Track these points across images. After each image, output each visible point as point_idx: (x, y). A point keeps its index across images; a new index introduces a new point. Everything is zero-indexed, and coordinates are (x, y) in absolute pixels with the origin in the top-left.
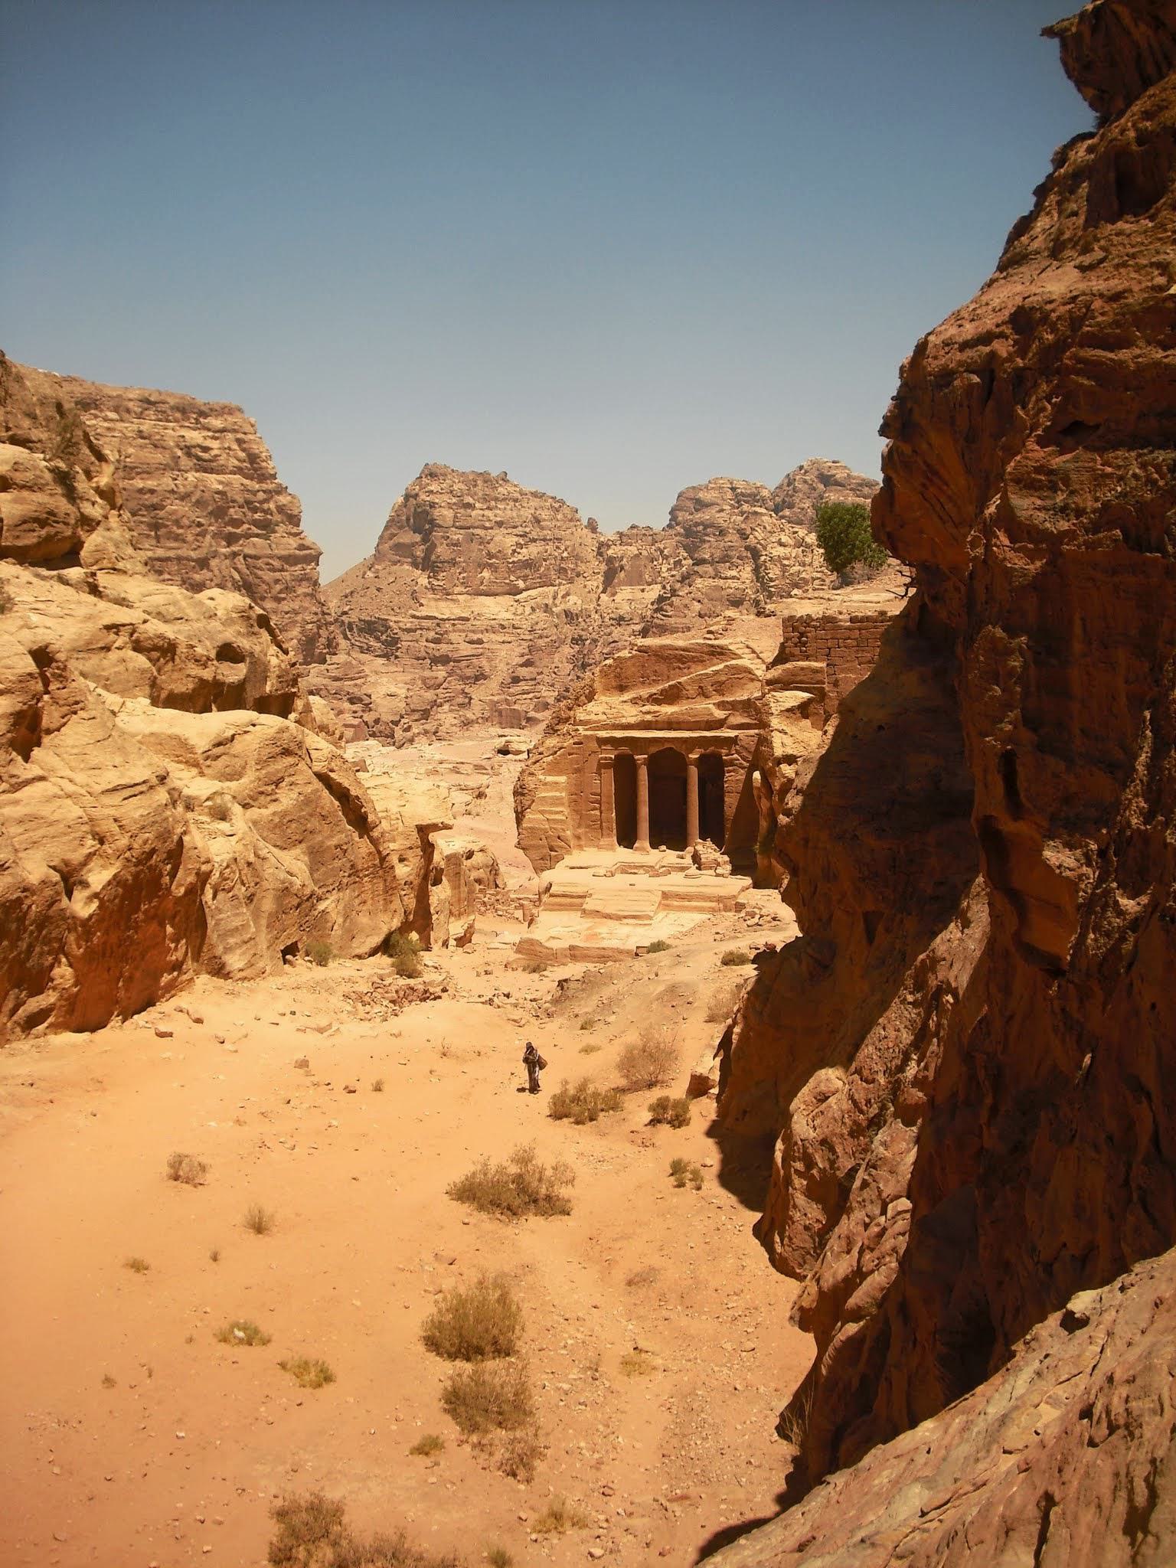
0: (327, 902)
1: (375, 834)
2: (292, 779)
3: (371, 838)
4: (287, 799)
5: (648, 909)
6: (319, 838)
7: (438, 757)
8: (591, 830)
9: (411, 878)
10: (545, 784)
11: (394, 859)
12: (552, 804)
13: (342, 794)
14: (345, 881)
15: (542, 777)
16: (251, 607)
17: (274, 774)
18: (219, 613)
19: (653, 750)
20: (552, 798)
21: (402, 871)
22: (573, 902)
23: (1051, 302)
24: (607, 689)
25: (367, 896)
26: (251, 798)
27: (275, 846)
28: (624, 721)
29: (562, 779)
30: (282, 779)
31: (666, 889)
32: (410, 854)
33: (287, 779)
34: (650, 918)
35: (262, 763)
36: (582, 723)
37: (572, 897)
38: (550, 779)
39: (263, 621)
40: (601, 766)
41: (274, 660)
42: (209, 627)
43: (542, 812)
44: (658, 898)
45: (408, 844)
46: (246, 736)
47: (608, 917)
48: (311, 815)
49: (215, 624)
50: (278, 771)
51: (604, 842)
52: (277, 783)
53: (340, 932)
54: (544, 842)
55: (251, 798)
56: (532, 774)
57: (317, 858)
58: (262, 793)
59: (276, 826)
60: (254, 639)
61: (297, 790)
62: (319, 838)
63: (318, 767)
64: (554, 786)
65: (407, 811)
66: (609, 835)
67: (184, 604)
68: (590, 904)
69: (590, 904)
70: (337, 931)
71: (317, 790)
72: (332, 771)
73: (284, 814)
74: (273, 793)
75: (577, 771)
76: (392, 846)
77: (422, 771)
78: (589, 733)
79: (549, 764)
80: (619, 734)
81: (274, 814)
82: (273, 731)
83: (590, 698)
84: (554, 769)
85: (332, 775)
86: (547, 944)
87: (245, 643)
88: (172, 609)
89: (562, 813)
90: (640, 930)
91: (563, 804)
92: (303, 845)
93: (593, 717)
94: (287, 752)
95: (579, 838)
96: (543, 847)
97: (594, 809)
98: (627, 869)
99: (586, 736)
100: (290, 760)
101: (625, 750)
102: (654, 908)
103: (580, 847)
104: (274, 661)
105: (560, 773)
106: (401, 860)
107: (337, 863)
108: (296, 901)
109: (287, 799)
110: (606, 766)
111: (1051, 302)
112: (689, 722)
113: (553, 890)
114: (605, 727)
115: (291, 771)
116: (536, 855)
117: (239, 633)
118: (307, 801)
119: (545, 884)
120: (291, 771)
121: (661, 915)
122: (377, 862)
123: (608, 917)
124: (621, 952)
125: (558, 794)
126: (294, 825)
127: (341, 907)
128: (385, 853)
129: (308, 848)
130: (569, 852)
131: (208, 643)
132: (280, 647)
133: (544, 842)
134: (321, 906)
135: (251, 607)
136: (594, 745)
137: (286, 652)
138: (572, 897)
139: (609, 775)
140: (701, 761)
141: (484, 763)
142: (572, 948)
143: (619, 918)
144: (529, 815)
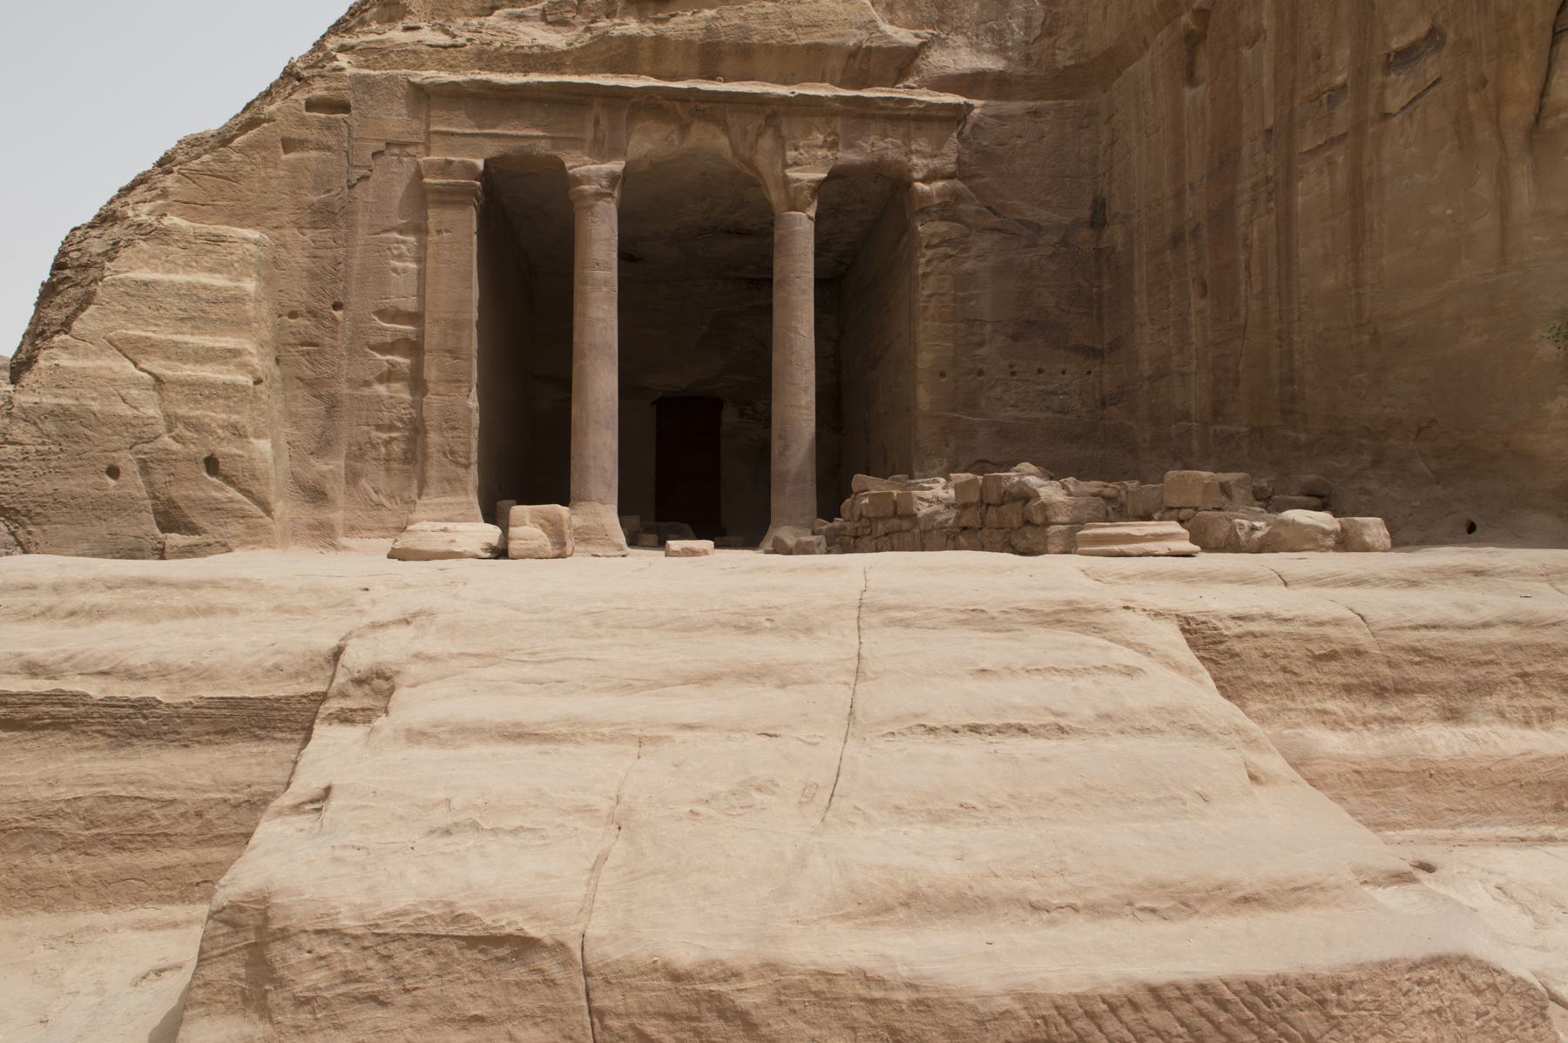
19: (647, 142)
20: (190, 293)
37: (132, 723)
40: (422, 197)
43: (130, 349)
54: (133, 484)
66: (451, 484)
75: (325, 216)
95: (316, 494)
97: (388, 376)
101: (524, 135)
110: (447, 197)
112: (787, 50)
130: (256, 536)
136: (396, 120)
138: (132, 723)
139: (458, 236)
140: (837, 194)
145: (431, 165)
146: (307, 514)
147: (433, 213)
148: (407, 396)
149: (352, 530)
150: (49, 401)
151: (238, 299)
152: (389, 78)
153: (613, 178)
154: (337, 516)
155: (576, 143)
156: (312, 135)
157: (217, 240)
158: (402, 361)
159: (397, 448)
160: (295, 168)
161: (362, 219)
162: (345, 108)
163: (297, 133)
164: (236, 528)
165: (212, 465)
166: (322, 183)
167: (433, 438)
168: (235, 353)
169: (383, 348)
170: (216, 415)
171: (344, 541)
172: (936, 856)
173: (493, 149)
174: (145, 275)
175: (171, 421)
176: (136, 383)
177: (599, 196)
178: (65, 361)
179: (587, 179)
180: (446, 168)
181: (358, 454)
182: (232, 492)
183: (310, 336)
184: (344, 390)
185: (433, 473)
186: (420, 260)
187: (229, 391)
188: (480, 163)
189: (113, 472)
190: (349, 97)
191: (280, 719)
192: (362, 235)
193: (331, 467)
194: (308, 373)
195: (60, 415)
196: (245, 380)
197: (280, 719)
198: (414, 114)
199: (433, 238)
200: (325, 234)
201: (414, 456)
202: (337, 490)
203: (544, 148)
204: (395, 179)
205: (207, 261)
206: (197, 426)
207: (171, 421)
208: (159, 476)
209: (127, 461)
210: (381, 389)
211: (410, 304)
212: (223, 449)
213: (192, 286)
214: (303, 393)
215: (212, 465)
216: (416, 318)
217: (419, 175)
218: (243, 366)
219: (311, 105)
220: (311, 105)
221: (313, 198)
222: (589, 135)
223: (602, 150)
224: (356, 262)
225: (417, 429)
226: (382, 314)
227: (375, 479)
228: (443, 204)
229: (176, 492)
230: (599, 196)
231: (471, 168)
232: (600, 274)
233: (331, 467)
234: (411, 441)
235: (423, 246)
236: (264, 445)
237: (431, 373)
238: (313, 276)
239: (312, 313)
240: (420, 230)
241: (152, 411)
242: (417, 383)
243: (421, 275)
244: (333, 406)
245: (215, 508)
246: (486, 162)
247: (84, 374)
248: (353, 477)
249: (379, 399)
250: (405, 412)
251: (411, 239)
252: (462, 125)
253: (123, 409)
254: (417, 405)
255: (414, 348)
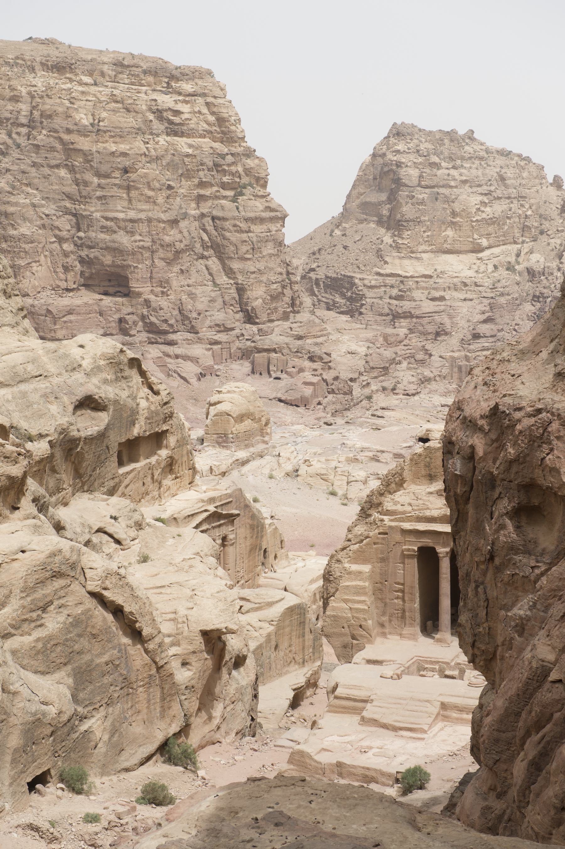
0: (93, 720)
1: (151, 646)
2: (62, 601)
3: (146, 651)
4: (53, 623)
5: (424, 722)
6: (87, 657)
7: (359, 445)
8: (392, 619)
9: (193, 682)
10: (350, 573)
11: (175, 665)
12: (358, 594)
13: (117, 611)
14: (116, 695)
15: (347, 565)
16: (122, 351)
17: (39, 600)
18: (85, 363)
20: (355, 587)
21: (183, 676)
22: (353, 705)
23: (520, 409)
24: (417, 478)
25: (142, 706)
26: (13, 626)
27: (36, 672)
28: (428, 513)
29: (366, 568)
30: (51, 602)
31: (446, 700)
32: (193, 659)
33: (56, 603)
34: (425, 732)
35: (27, 590)
36: (388, 513)
37: (355, 700)
38: (355, 567)
39: (135, 363)
41: (145, 403)
42: (69, 382)
43: (346, 601)
44: (435, 709)
45: (191, 648)
46: (15, 565)
47: (385, 726)
48: (80, 636)
49: (79, 376)
50: (45, 596)
51: (407, 631)
52: (44, 609)
53: (104, 750)
54: (347, 630)
55: (13, 626)
56: (338, 561)
57: (83, 677)
58: (26, 620)
59: (38, 653)
60: (123, 384)
61: (66, 612)
62: (87, 657)
63: (92, 586)
64: (359, 574)
65: (193, 614)
66: (411, 625)
67: (45, 359)
68: (370, 712)
69: (370, 712)
70: (102, 748)
71: (89, 610)
72: (105, 589)
73: (50, 638)
74: (39, 618)
75: (383, 560)
76: (173, 651)
77: (342, 459)
78: (393, 524)
79: (354, 552)
80: (422, 527)
81: (38, 640)
82: (41, 557)
83: (401, 484)
84: (360, 558)
85: (105, 593)
86: (316, 758)
87: (107, 392)
88: (30, 367)
89: (365, 602)
90: (411, 746)
91: (365, 594)
92: (69, 667)
93: (399, 508)
94: (58, 575)
95: (382, 625)
96: (344, 635)
97: (397, 598)
98: (421, 668)
99: (390, 527)
100: (59, 583)
101: (427, 542)
102: (430, 720)
103: (384, 635)
104: (143, 404)
105: (365, 561)
106: (184, 664)
107: (107, 680)
108: (49, 730)
109: (53, 623)
110: (410, 557)
111: (520, 409)
113: (339, 692)
114: (409, 519)
115: (62, 593)
116: (338, 642)
117: (105, 381)
118: (78, 623)
119: (332, 684)
120: (62, 593)
121: (440, 725)
122: (154, 671)
123: (385, 726)
124: (383, 774)
125: (361, 583)
126: (59, 649)
127: (108, 723)
128: (161, 663)
129: (73, 670)
130: (370, 642)
131: (65, 399)
132: (151, 388)
133: (347, 630)
134: (84, 727)
135: (122, 351)
136: (398, 537)
137: (157, 393)
138: (355, 700)
141: (403, 452)
142: (339, 765)
143: (395, 729)
144: (333, 603)
145: (405, 549)
146: (380, 630)
147: (406, 560)
148: (401, 603)
149: (390, 633)
150: (332, 613)
151: (365, 588)
152: (397, 526)
153: (447, 553)
154: (387, 631)
155: (438, 544)
156: (380, 541)
157: (360, 573)
158: (400, 594)
159: (400, 615)
160: (377, 549)
161: (391, 560)
162: (386, 534)
163: (377, 541)
164: (365, 640)
165: (361, 626)
166: (382, 553)
167: (407, 614)
168: (365, 601)
169: (396, 591)
170: (361, 616)
171: (388, 636)
172: (399, 718)
173: (420, 545)
174: (347, 584)
175: (353, 617)
176: (347, 609)
177: (444, 557)
178: (334, 604)
179: (441, 553)
180: (409, 550)
181: (391, 616)
182: (365, 633)
183: (380, 589)
184: (388, 601)
185: (407, 622)
186: (404, 570)
187: (364, 610)
188: (416, 549)
189: (343, 627)
190: (388, 531)
191: (365, 701)
192: (391, 564)
193: (385, 619)
194: (380, 597)
195: (334, 616)
196: (366, 608)
197: (365, 701)
198: (402, 535)
199: (406, 566)
200: (383, 564)
201: (403, 617)
202: (387, 624)
203: (431, 545)
204: (397, 551)
205: (359, 578)
206: (358, 618)
207: (353, 617)
208: (351, 629)
209: (345, 625)
210: (396, 601)
211: (402, 581)
212: (363, 623)
213: (356, 585)
214: (379, 601)
215: (361, 626)
216: (403, 584)
217: (403, 551)
218: (366, 604)
219: (379, 534)
220: (379, 534)
221: (380, 556)
222: (441, 541)
223: (444, 546)
224: (390, 570)
225: (404, 611)
226: (396, 583)
227: (395, 622)
228: (408, 558)
229: (355, 632)
230: (444, 557)
231: (414, 550)
232: (444, 576)
233: (385, 619)
234: (403, 613)
235: (404, 567)
236: (370, 622)
237: (406, 598)
238: (381, 574)
239: (381, 583)
240: (403, 563)
241: (350, 615)
242: (404, 601)
243: (404, 573)
244: (386, 604)
245: (362, 636)
246: (419, 548)
247: (337, 607)
248: (390, 621)
249: (395, 603)
250: (401, 607)
251: (402, 565)
252: (412, 538)
253: (345, 615)
254: (403, 605)
255: (403, 591)
